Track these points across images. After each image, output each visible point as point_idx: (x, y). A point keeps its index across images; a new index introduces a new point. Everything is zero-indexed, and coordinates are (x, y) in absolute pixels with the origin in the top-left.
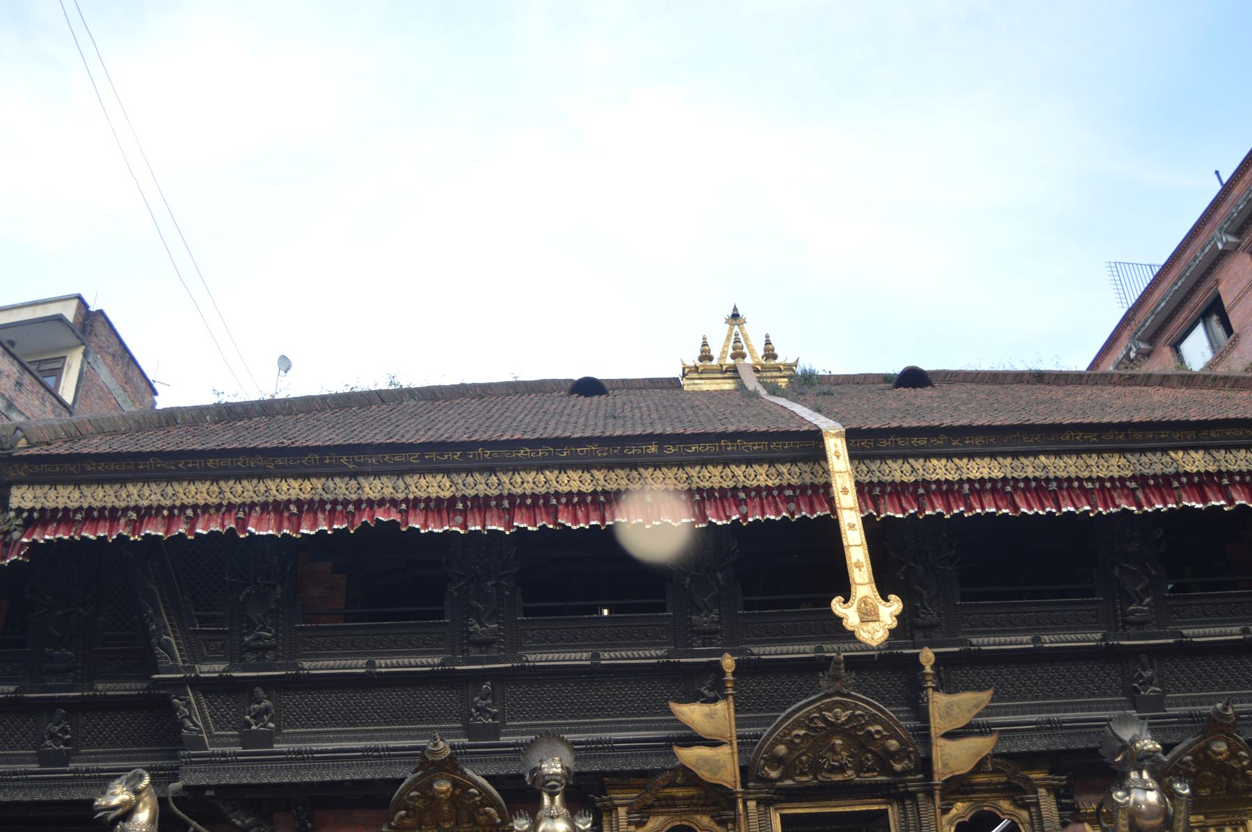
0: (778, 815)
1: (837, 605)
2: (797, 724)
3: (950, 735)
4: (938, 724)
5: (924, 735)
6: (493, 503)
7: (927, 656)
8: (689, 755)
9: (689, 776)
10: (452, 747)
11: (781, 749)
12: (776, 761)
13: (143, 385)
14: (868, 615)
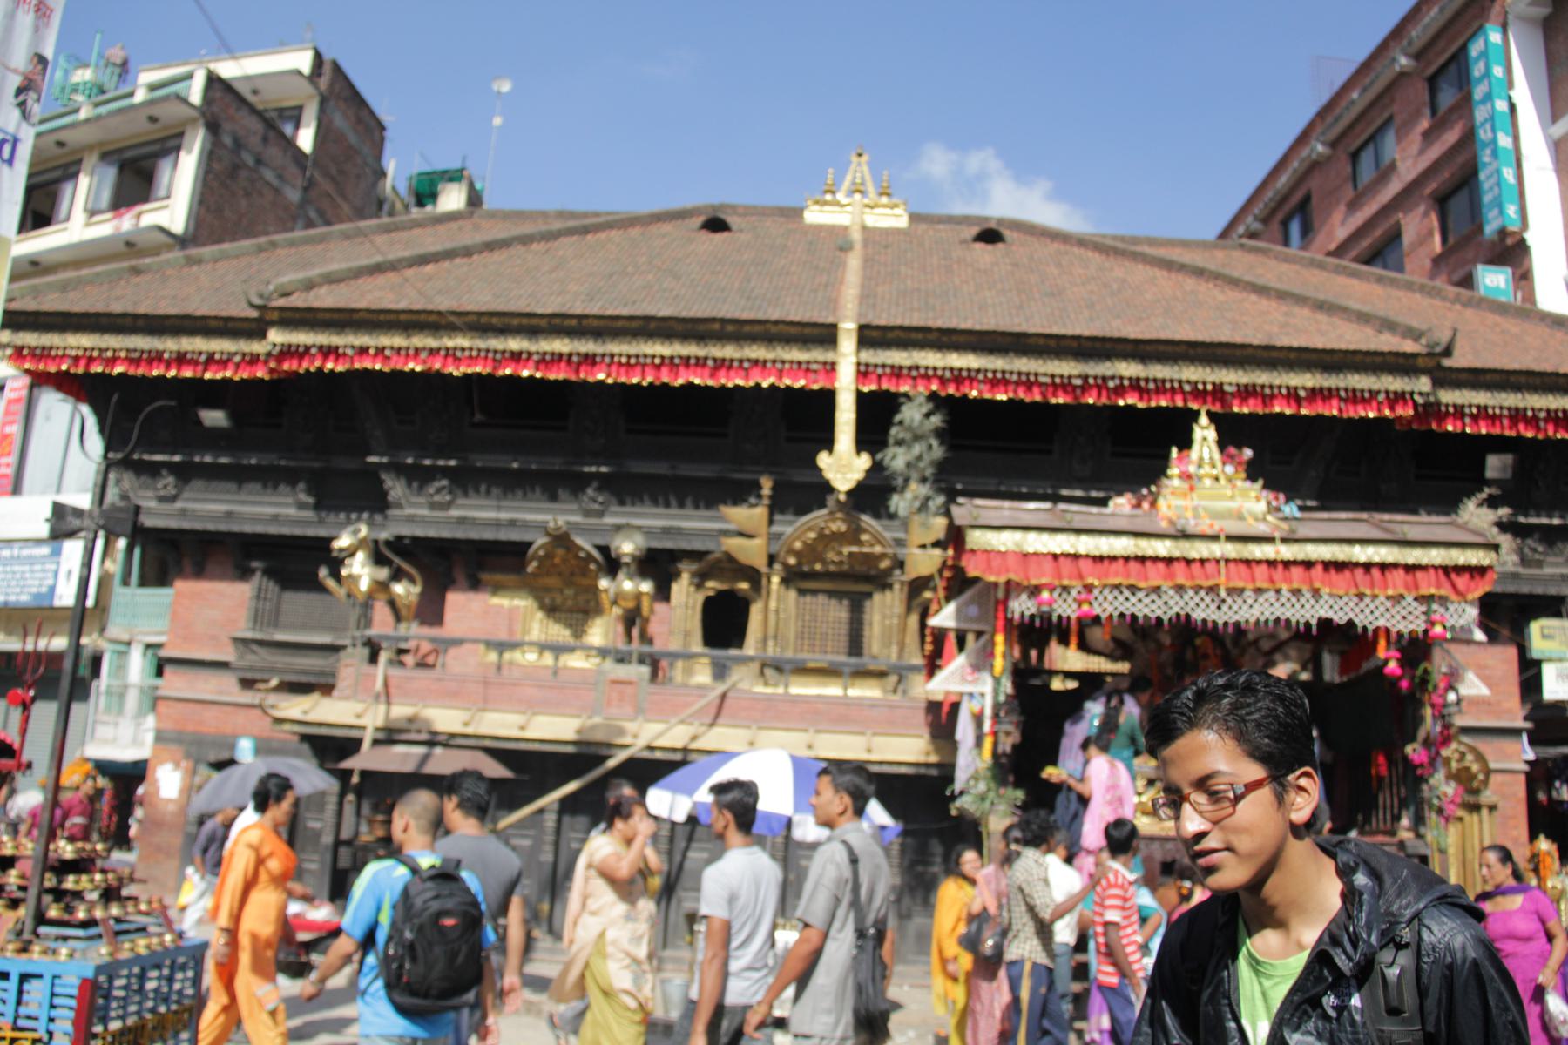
1: (823, 459)
2: (810, 529)
6: (598, 359)
9: (729, 558)
10: (568, 523)
11: (798, 545)
12: (791, 551)
13: (373, 123)
14: (844, 468)
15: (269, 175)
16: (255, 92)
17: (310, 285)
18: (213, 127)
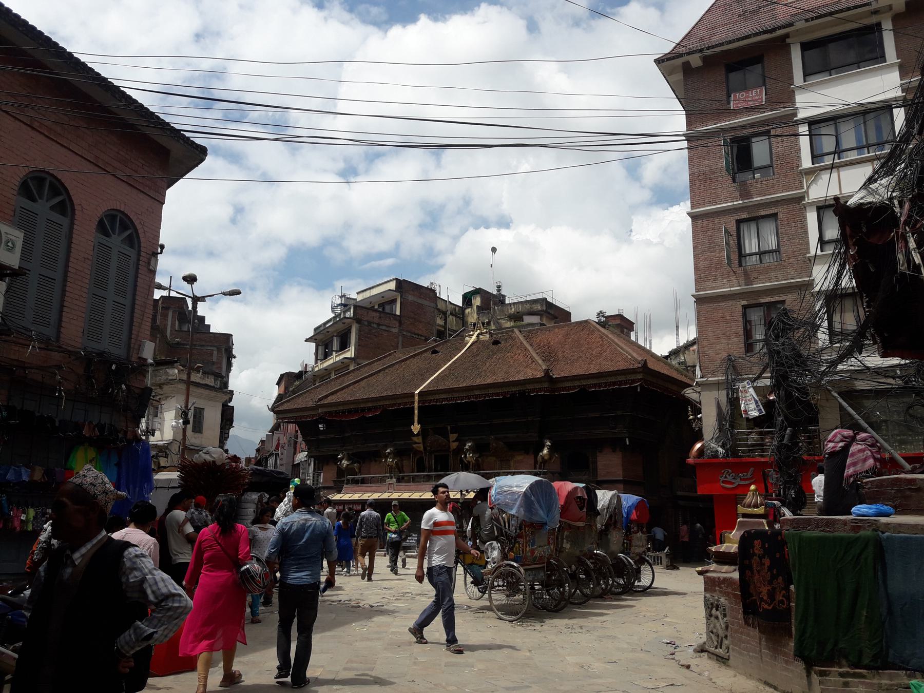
0: (433, 456)
1: (412, 427)
3: (454, 441)
4: (451, 440)
5: (449, 441)
7: (449, 428)
8: (414, 446)
15: (384, 328)
16: (383, 297)
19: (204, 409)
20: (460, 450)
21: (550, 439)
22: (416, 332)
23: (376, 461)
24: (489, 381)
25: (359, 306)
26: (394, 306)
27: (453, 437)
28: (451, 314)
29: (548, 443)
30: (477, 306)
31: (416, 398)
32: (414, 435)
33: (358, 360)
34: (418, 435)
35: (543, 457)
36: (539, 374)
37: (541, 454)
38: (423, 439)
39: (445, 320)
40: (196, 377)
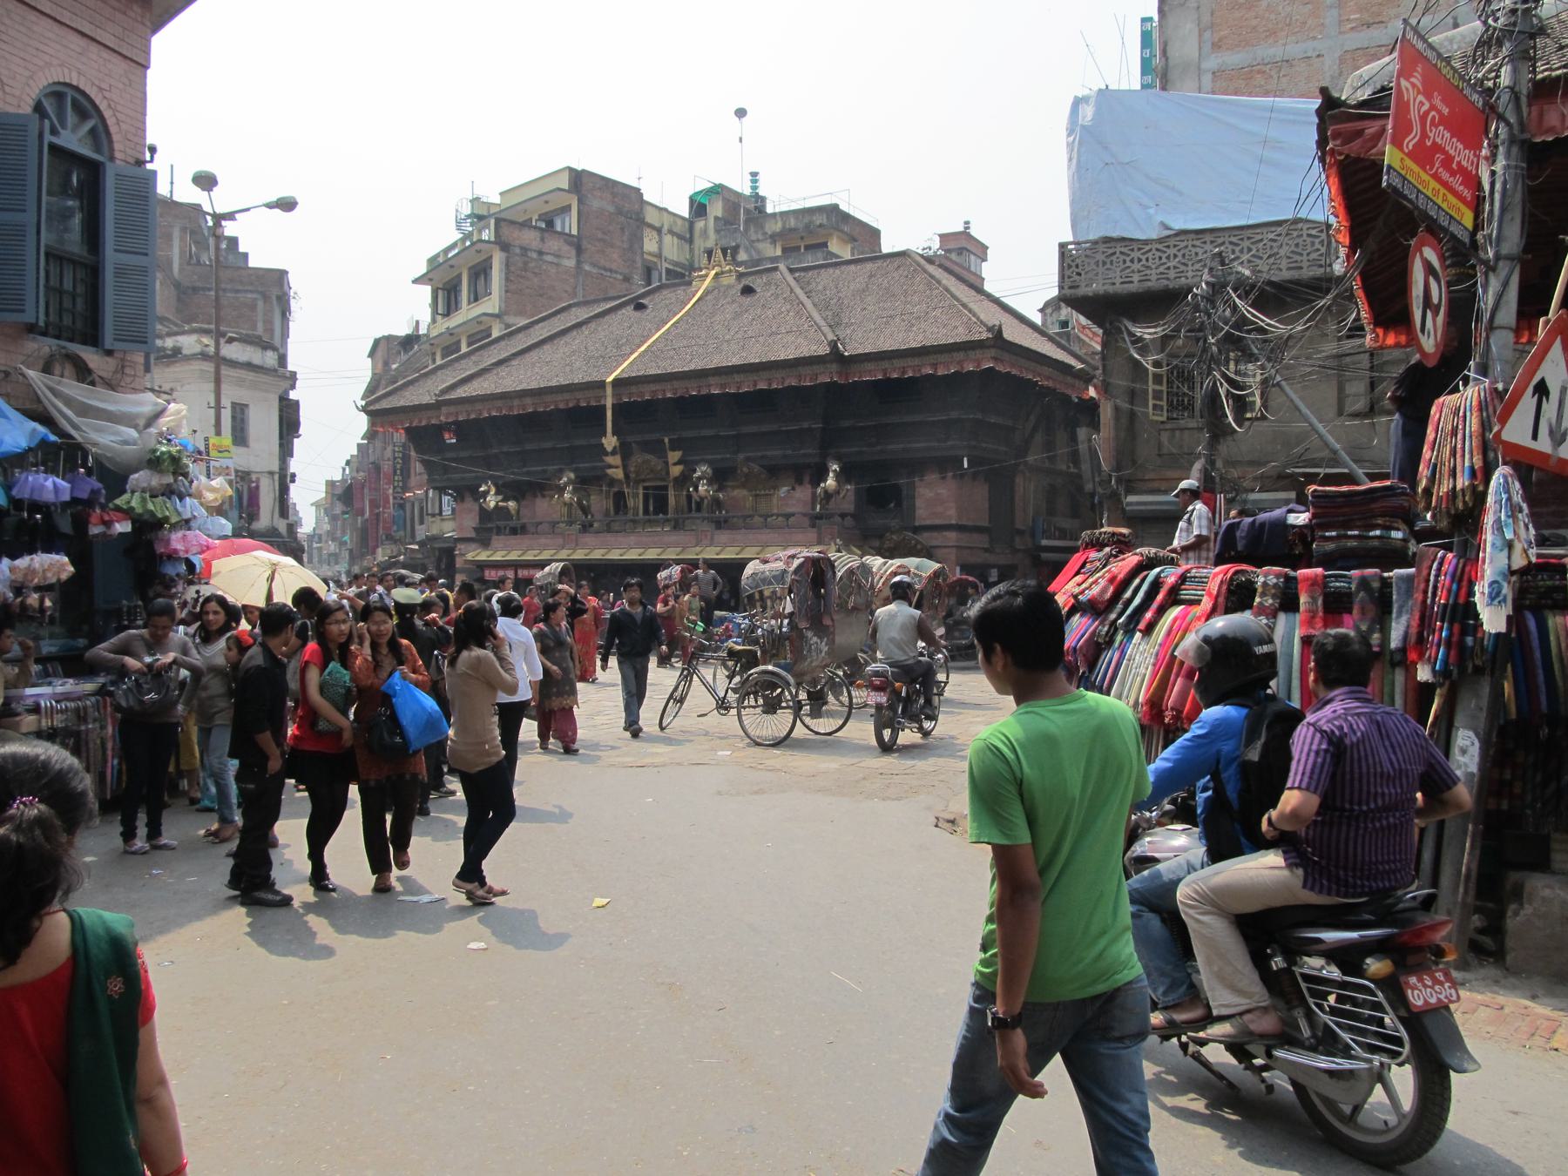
1: (604, 441)
3: (675, 464)
5: (667, 463)
7: (666, 440)
8: (610, 471)
15: (549, 258)
16: (547, 202)
17: (453, 387)
18: (505, 247)
19: (247, 406)
20: (685, 480)
21: (838, 459)
22: (608, 265)
23: (544, 496)
24: (735, 361)
25: (505, 220)
26: (567, 219)
27: (674, 456)
28: (670, 232)
29: (835, 467)
30: (716, 218)
31: (609, 390)
32: (607, 454)
33: (505, 317)
34: (614, 453)
35: (826, 491)
36: (824, 350)
37: (822, 485)
38: (623, 459)
39: (660, 242)
40: (232, 351)
